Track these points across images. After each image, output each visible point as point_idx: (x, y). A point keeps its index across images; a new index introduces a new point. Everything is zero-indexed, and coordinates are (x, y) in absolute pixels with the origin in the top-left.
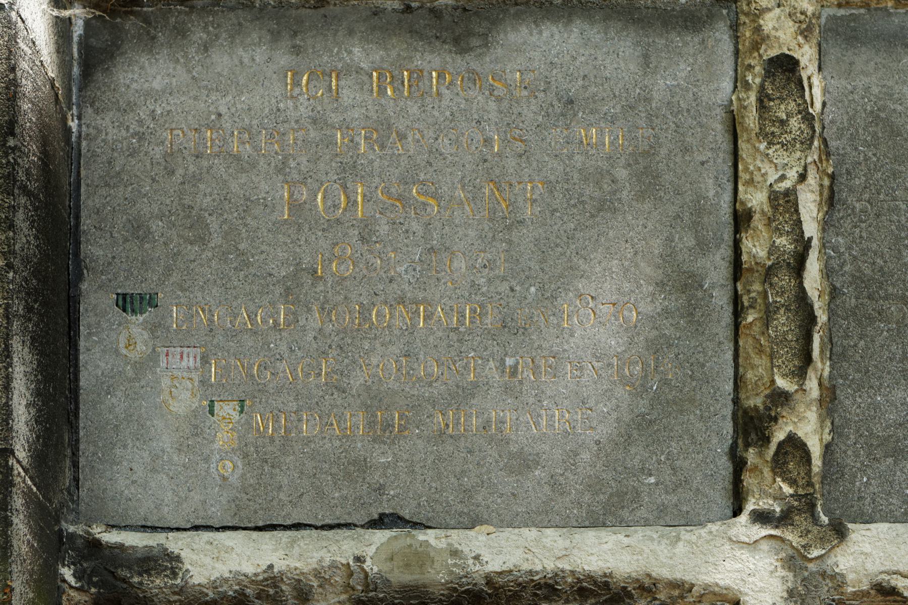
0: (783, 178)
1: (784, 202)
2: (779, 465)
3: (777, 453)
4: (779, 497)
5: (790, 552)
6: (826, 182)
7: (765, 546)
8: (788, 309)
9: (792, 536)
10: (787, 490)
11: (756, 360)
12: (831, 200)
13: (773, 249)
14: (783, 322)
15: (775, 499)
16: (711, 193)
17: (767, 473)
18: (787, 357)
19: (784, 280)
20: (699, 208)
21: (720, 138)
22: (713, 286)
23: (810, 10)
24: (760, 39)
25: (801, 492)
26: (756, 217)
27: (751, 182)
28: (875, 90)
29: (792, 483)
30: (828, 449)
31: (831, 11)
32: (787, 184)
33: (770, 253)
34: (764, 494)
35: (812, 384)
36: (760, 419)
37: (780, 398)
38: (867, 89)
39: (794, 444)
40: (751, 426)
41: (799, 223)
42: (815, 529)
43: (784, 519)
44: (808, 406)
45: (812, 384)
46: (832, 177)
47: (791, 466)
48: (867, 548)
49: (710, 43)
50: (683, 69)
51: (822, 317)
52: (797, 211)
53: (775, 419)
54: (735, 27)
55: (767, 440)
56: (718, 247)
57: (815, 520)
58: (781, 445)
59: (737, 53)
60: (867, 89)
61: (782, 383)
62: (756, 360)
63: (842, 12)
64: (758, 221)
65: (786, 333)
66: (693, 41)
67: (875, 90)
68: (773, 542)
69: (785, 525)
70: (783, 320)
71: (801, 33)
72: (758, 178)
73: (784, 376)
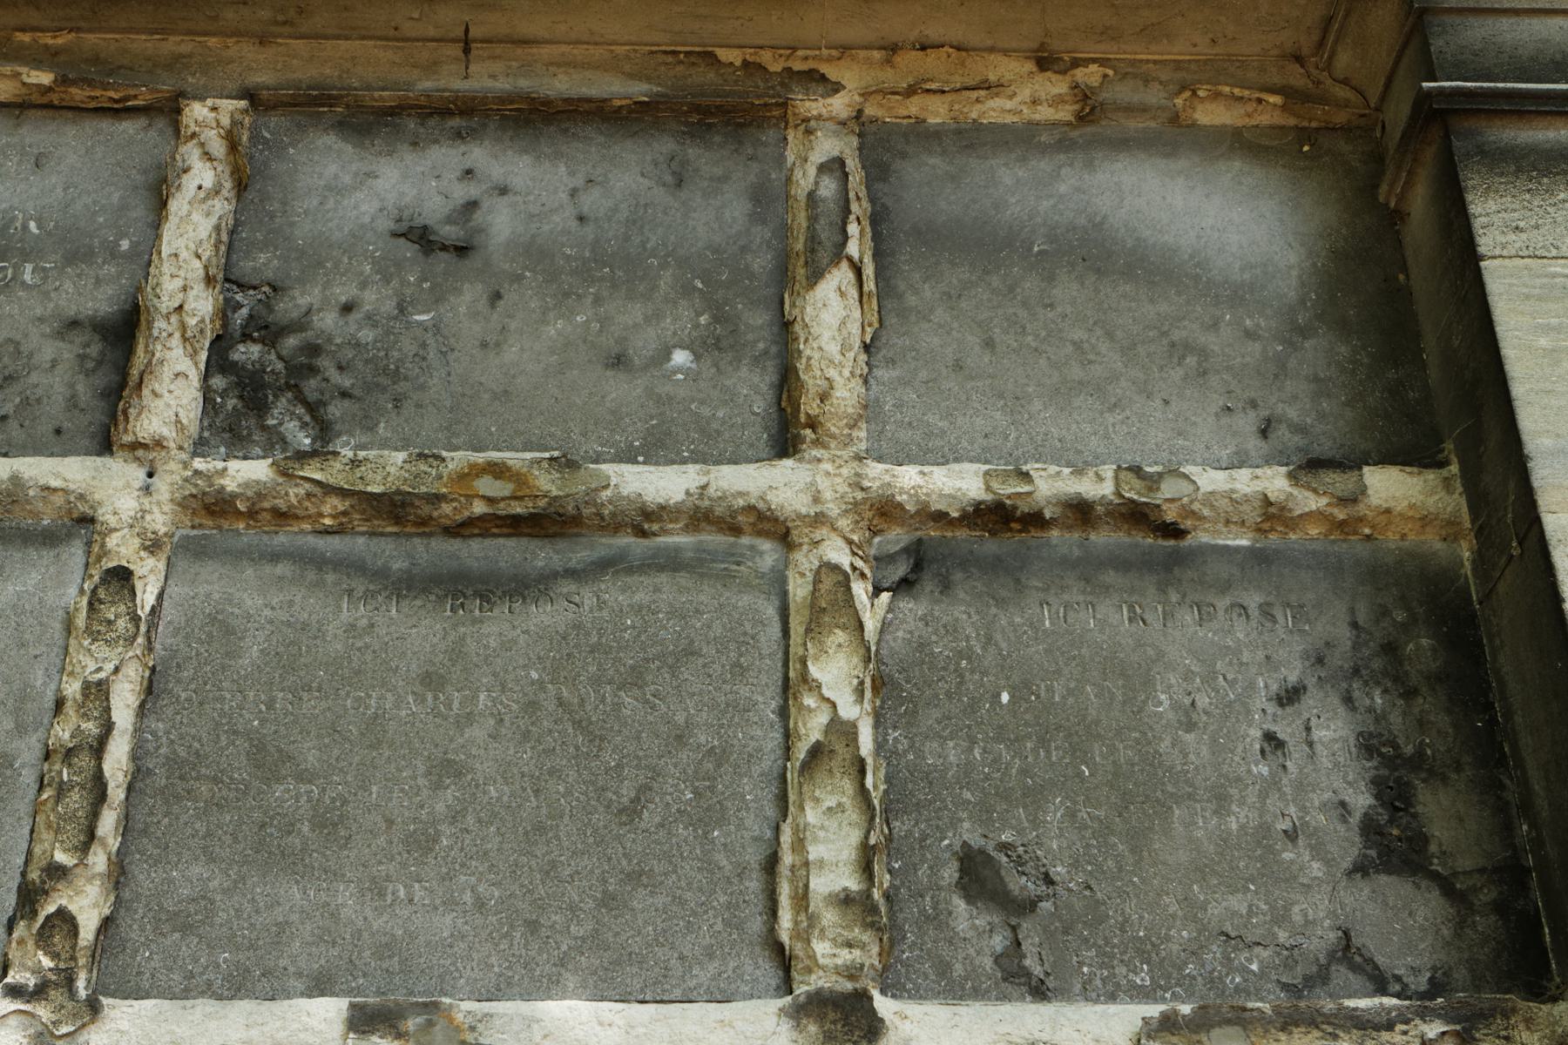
0: (100, 669)
1: (98, 691)
2: (43, 938)
3: (42, 927)
4: (37, 970)
5: (40, 1028)
6: (147, 674)
7: (13, 1021)
8: (83, 787)
9: (43, 1012)
10: (47, 963)
11: (45, 836)
12: (151, 690)
13: (77, 732)
14: (76, 800)
15: (33, 972)
16: (39, 683)
17: (31, 945)
18: (73, 834)
19: (84, 761)
20: (23, 697)
21: (57, 636)
22: (23, 766)
23: (163, 530)
24: (104, 552)
25: (62, 965)
26: (69, 704)
27: (71, 674)
28: (216, 596)
29: (55, 956)
30: (107, 924)
31: (184, 532)
32: (102, 675)
33: (72, 736)
34: (24, 967)
35: (99, 860)
36: (36, 892)
37: (57, 872)
38: (208, 595)
39: (64, 919)
40: (29, 897)
41: (108, 710)
42: (70, 1005)
43: (39, 993)
44: (90, 880)
45: (99, 860)
46: (153, 669)
47: (57, 939)
48: (124, 1025)
49: (64, 556)
50: (35, 577)
51: (116, 794)
52: (107, 699)
53: (46, 893)
54: (89, 544)
55: (35, 913)
56: (36, 730)
57: (72, 992)
58: (48, 918)
59: (87, 565)
60: (208, 595)
61: (61, 857)
62: (45, 836)
63: (195, 532)
64: (69, 708)
65: (76, 810)
66: (48, 555)
67: (216, 596)
68: (22, 1018)
69: (39, 1000)
70: (76, 797)
71: (146, 549)
72: (78, 669)
73: (65, 850)
